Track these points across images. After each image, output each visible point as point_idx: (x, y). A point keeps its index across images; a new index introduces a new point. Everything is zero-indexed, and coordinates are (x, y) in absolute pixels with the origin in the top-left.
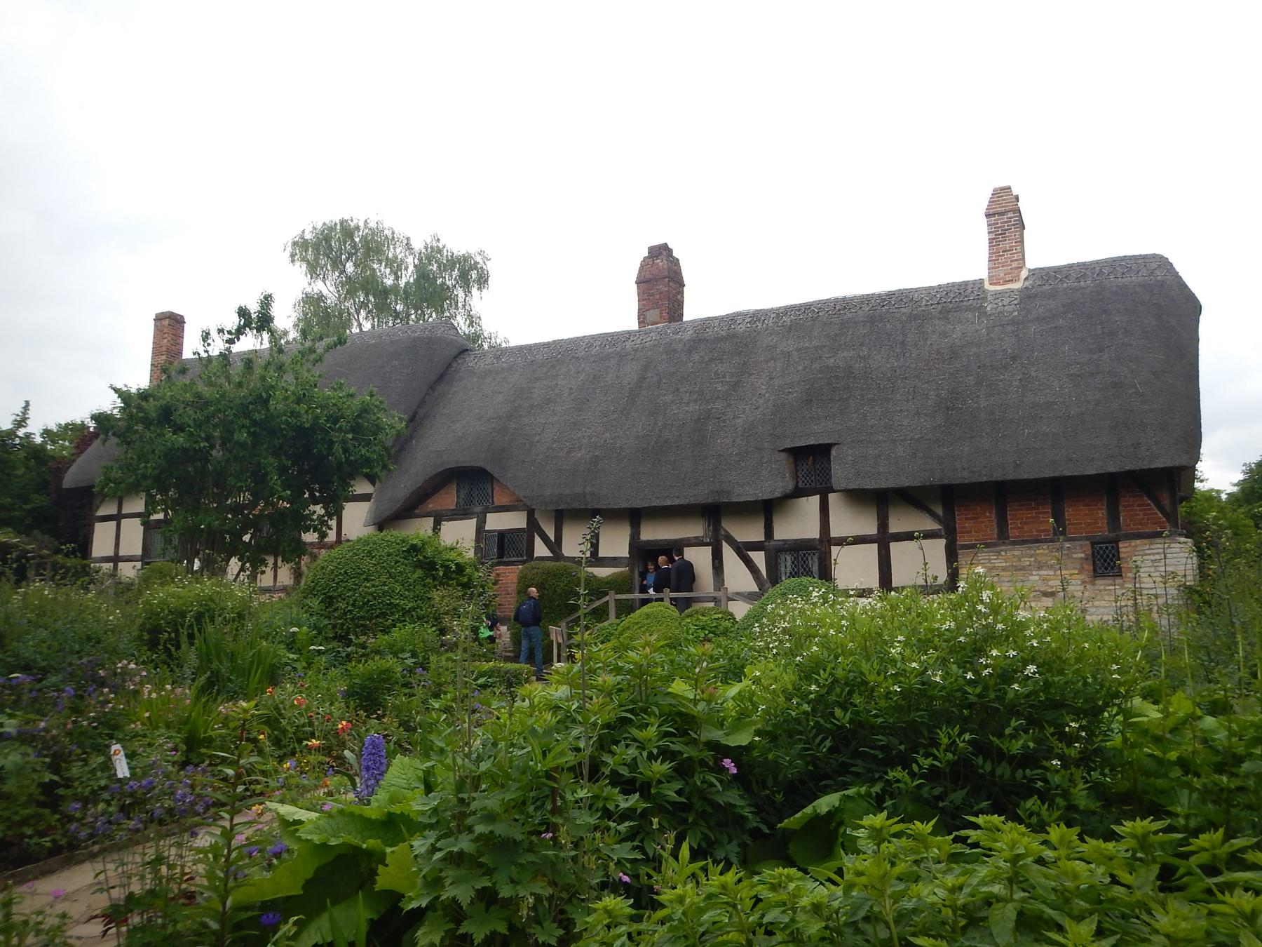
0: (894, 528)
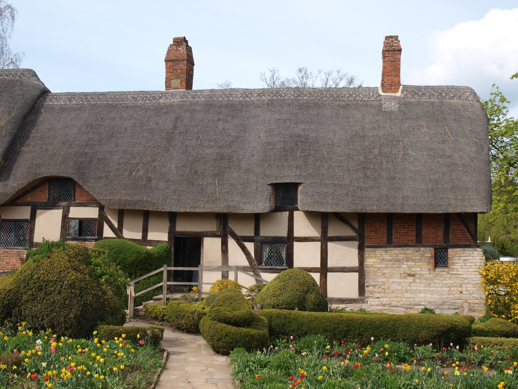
0: (330, 234)
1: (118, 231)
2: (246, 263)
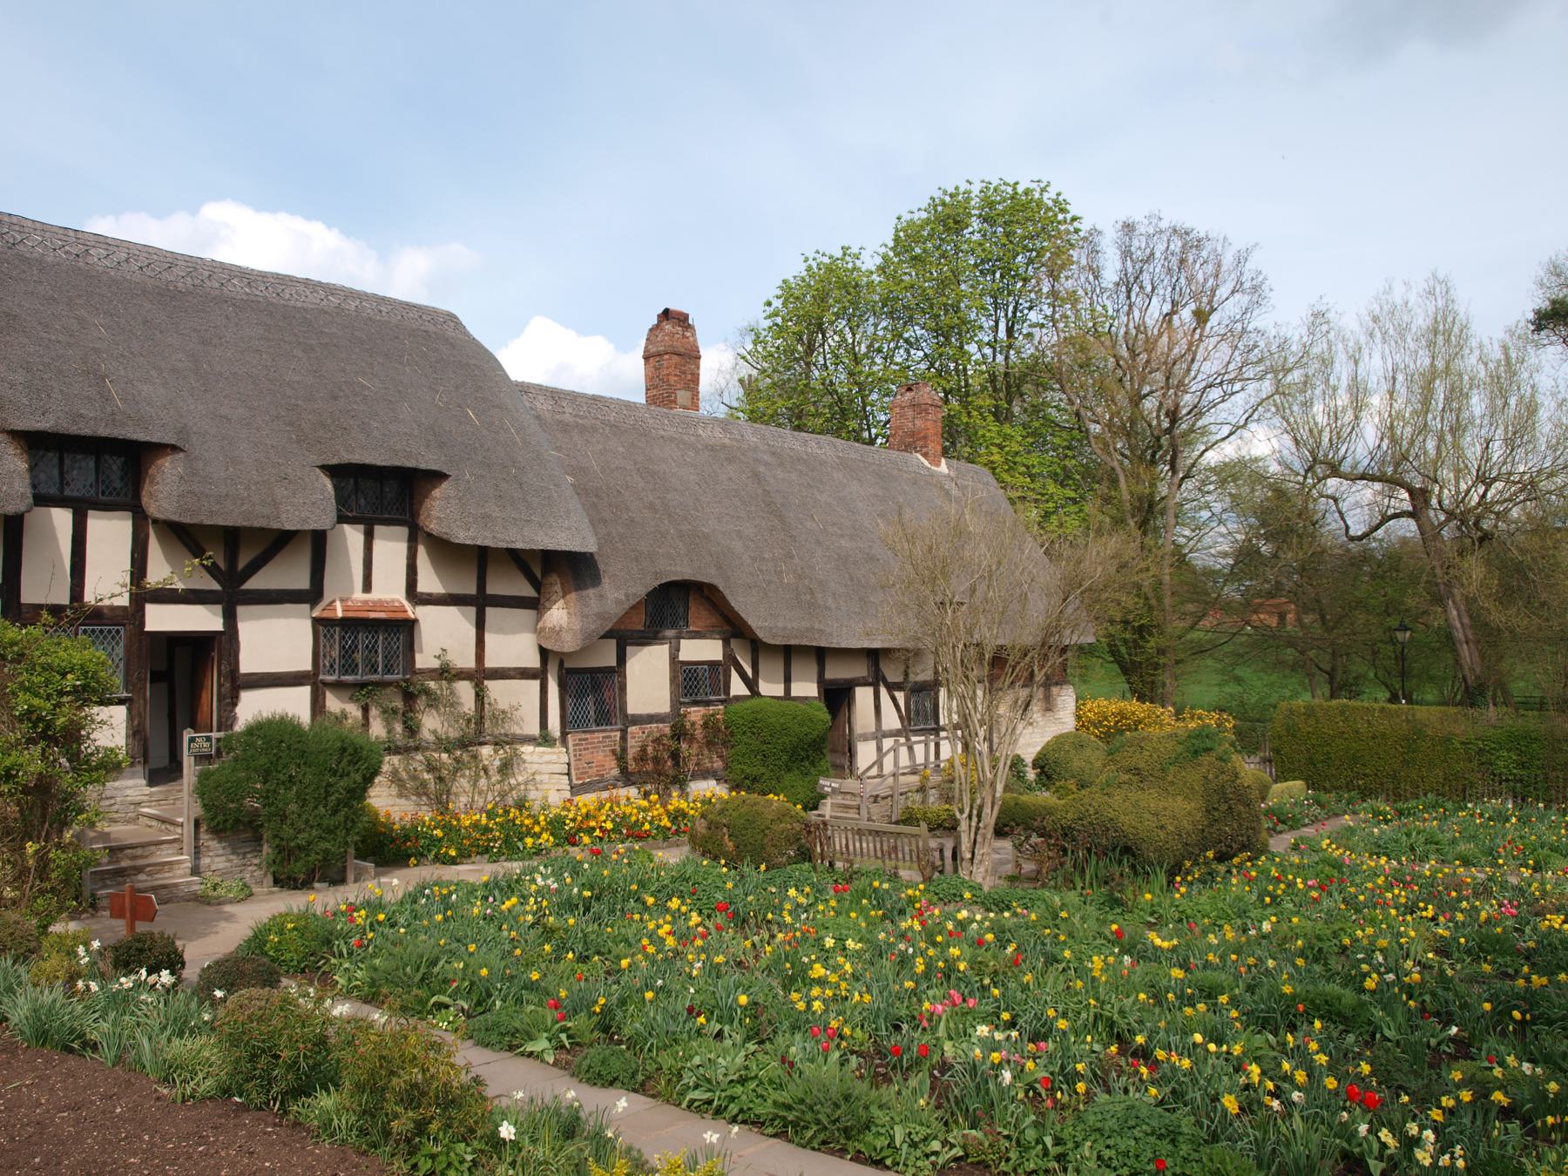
1: (751, 684)
2: (897, 725)
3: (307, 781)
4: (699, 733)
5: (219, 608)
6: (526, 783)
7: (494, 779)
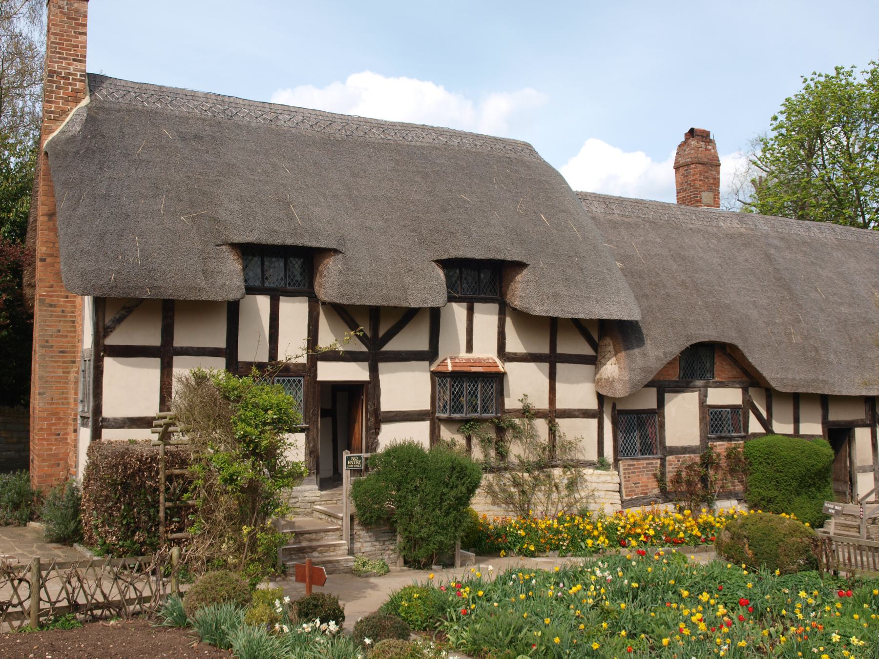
1: (766, 424)
3: (427, 491)
4: (723, 462)
5: (366, 364)
6: (587, 497)
7: (563, 494)
